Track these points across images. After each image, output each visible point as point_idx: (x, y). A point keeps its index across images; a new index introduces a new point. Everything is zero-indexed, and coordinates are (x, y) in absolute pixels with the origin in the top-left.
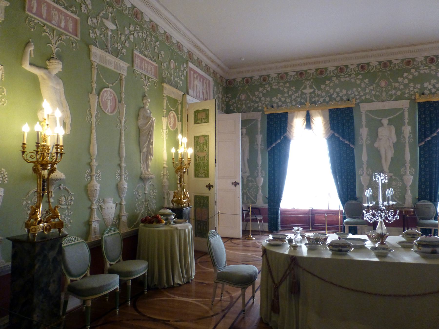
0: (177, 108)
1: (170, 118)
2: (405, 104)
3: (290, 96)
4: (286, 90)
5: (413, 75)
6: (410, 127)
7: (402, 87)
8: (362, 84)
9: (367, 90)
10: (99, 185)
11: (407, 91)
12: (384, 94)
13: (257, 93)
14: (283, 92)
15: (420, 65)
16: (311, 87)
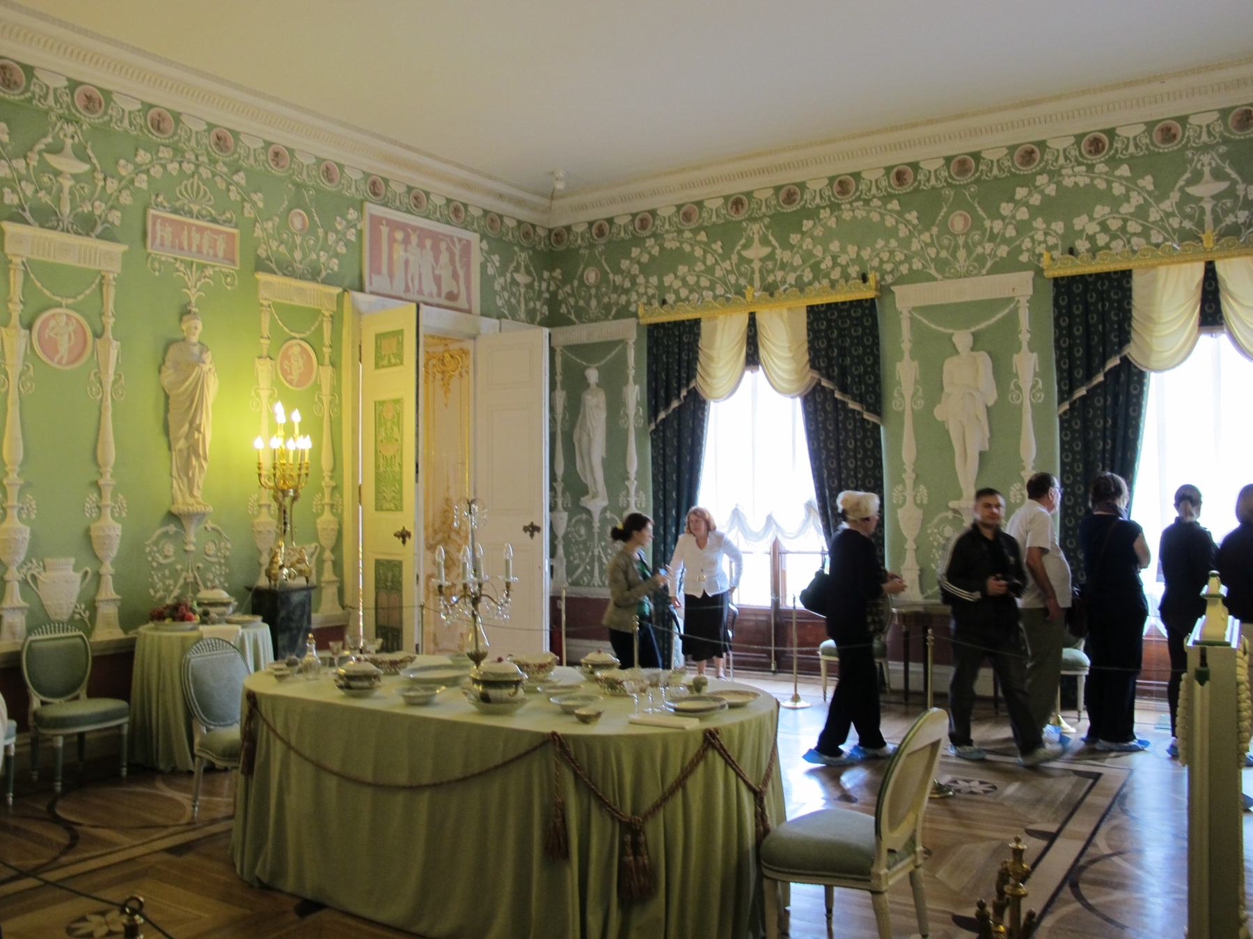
0: (320, 329)
1: (286, 356)
2: (1020, 285)
3: (710, 270)
4: (698, 252)
5: (1042, 192)
6: (1035, 355)
7: (1011, 232)
8: (901, 226)
9: (915, 246)
10: (28, 529)
11: (1027, 244)
12: (962, 254)
13: (625, 264)
14: (689, 260)
15: (1061, 160)
16: (765, 241)
